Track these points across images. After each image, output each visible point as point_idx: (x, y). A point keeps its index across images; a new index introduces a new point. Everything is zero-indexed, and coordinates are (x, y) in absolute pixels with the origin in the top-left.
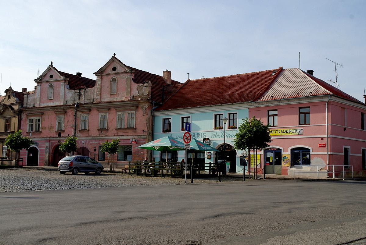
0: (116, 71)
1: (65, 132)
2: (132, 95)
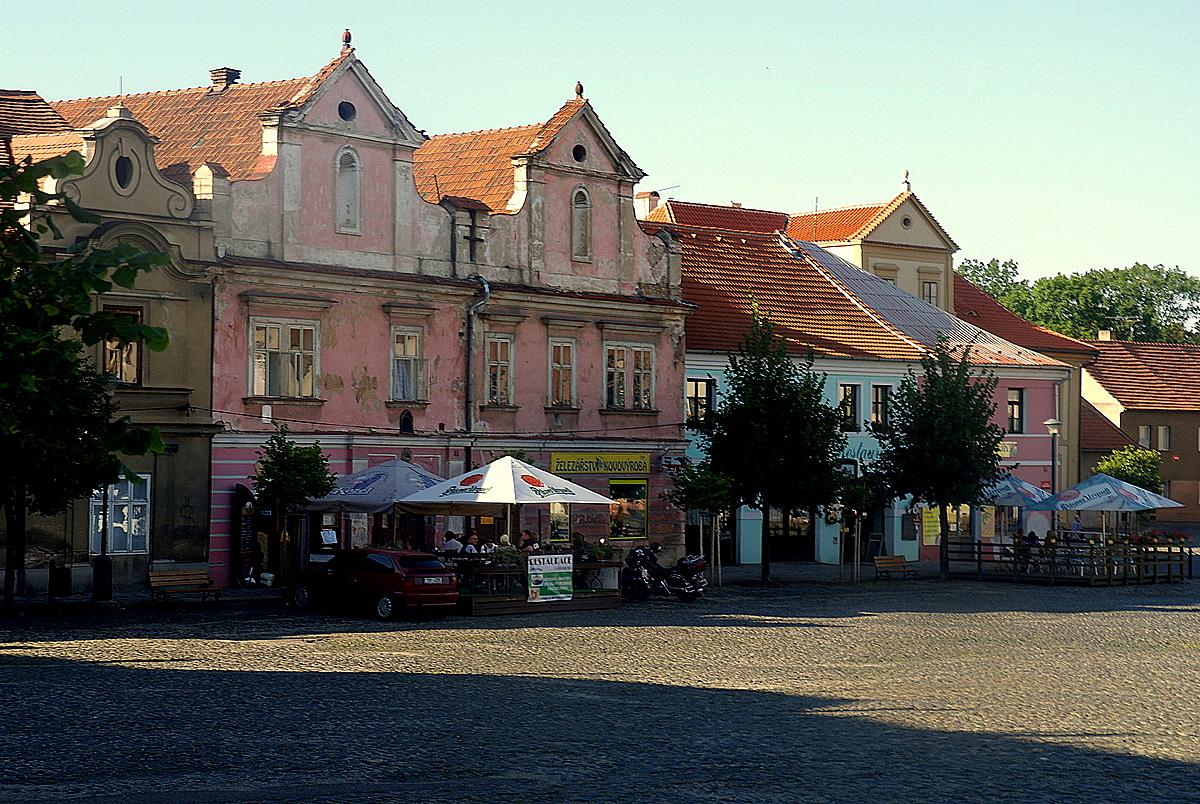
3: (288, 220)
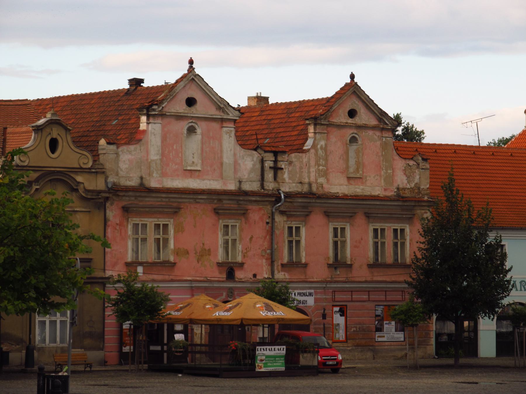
0: (357, 120)
1: (245, 266)
2: (395, 185)
3: (153, 165)
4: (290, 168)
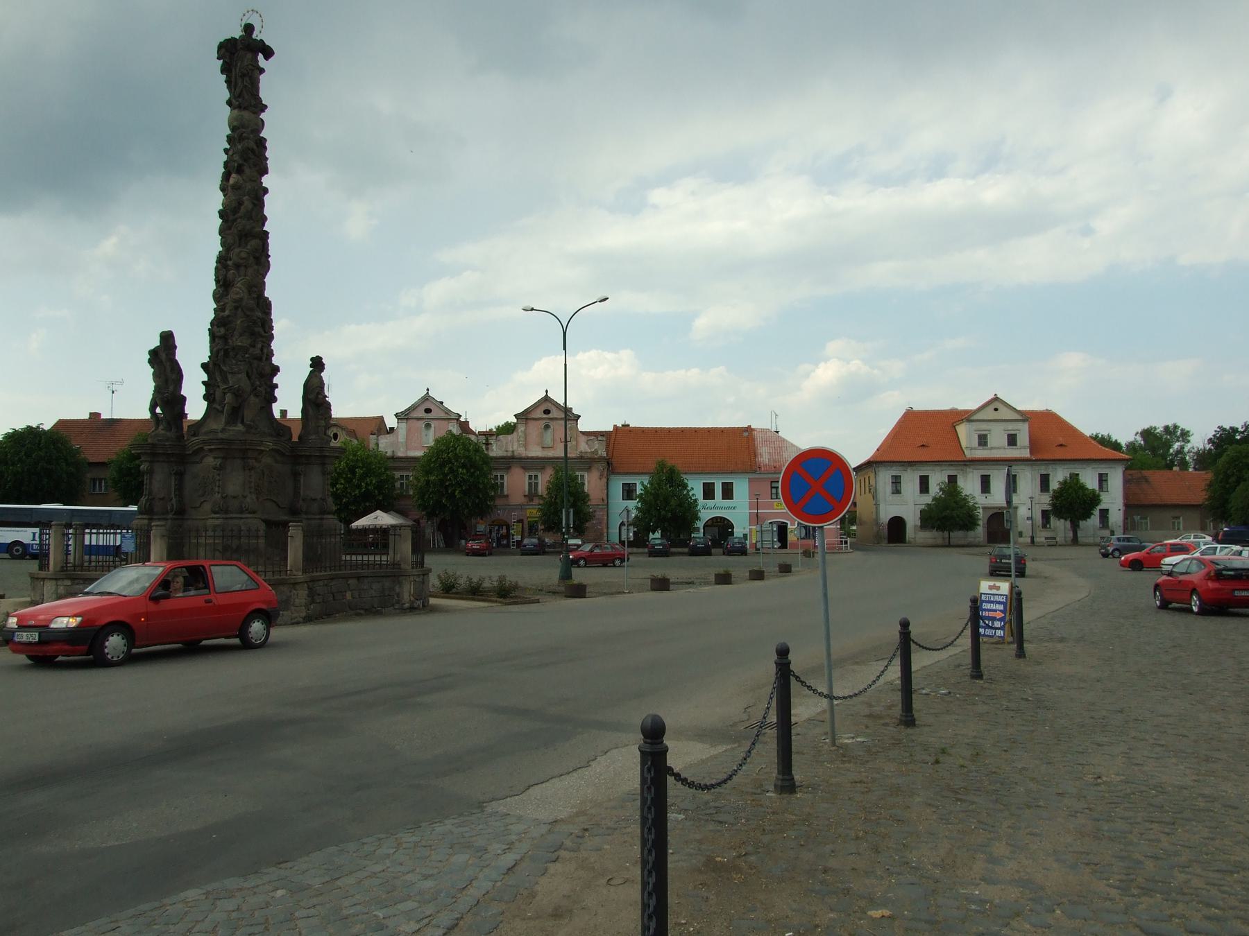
0: (550, 416)
4: (499, 443)
